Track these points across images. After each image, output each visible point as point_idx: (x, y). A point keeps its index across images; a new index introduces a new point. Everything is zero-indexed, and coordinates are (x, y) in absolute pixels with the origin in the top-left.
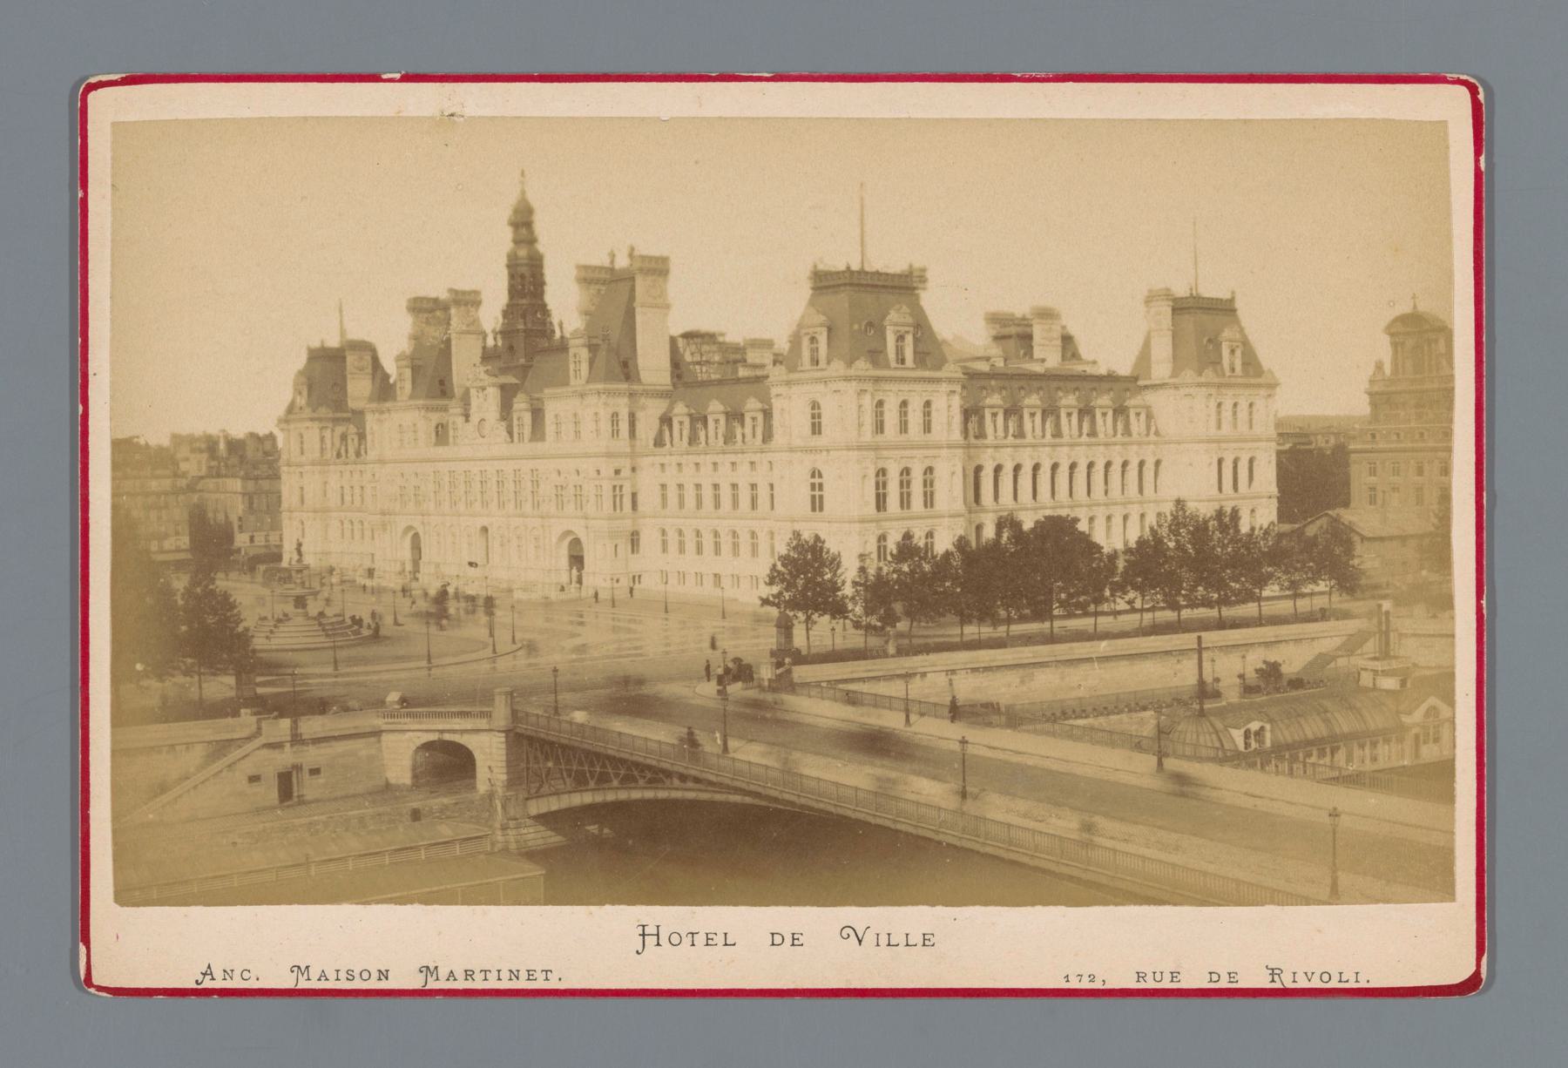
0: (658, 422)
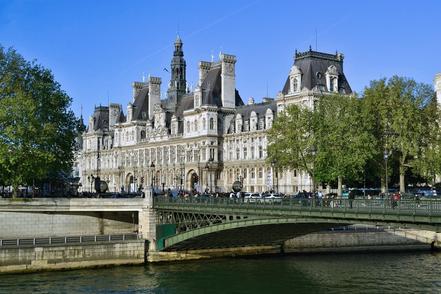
0: (230, 123)
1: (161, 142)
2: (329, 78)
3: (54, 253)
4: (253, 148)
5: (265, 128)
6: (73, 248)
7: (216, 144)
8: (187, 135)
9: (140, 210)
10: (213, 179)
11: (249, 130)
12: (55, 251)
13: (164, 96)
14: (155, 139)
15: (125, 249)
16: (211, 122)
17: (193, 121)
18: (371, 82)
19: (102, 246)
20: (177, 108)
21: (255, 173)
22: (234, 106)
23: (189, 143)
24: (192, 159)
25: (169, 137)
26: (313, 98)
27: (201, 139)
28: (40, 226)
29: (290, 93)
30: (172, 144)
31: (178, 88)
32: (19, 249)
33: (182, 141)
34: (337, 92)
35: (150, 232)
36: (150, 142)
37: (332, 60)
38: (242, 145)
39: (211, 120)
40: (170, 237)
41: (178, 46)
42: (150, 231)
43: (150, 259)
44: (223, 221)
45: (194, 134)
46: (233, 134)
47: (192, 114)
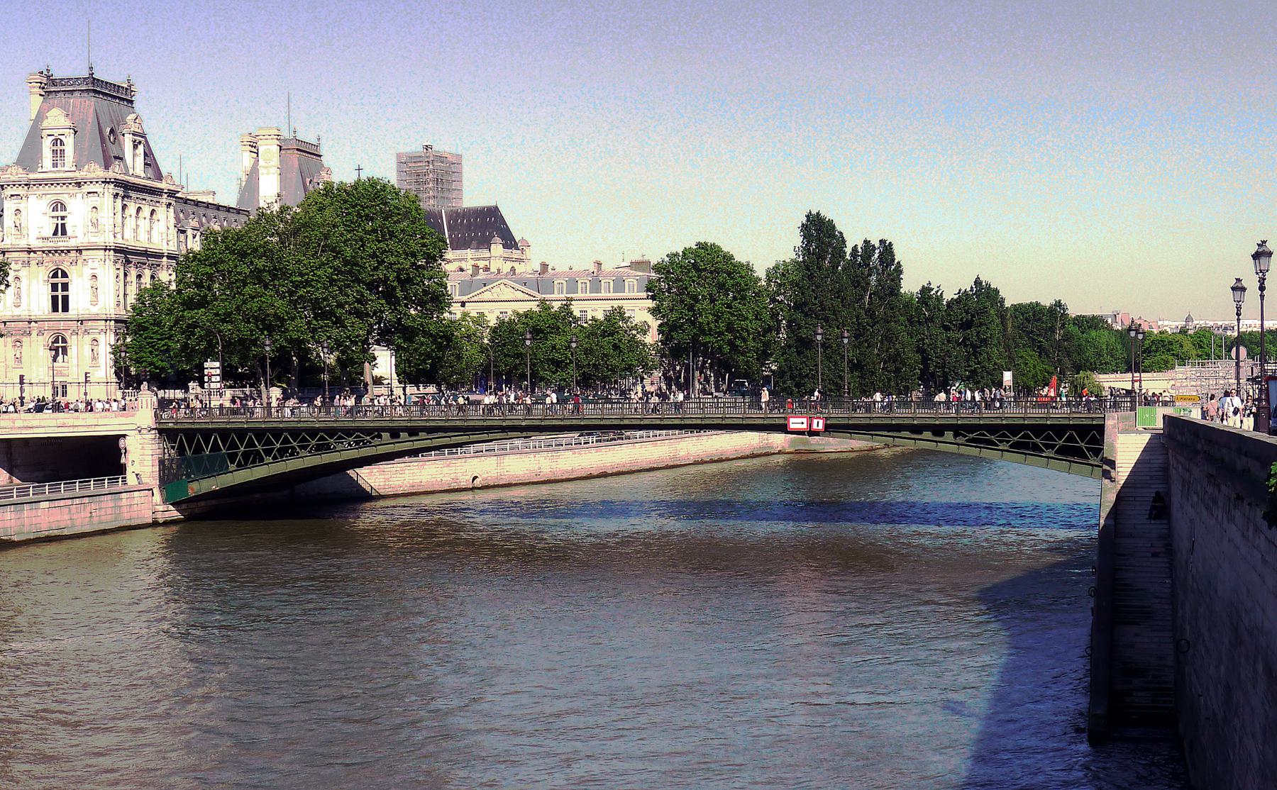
29: (43, 170)
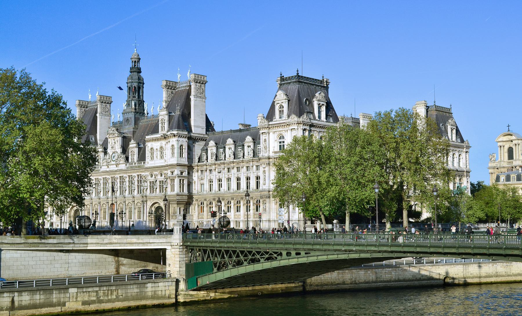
1: (116, 171)
2: (317, 105)
3: (88, 294)
4: (229, 179)
5: (244, 157)
6: (106, 288)
7: (185, 174)
8: (149, 163)
9: (168, 247)
10: (182, 213)
11: (225, 159)
12: (89, 292)
13: (117, 116)
14: (108, 167)
15: (157, 289)
16: (180, 149)
17: (158, 148)
18: (376, 113)
19: (135, 286)
20: (134, 132)
21: (232, 207)
22: (204, 131)
23: (152, 172)
24: (156, 191)
25: (126, 165)
26: (302, 127)
27: (169, 169)
28: (56, 266)
29: (276, 120)
30: (131, 173)
31: (135, 109)
32: (54, 290)
33: (144, 170)
34: (325, 120)
35: (180, 271)
36: (102, 170)
37: (319, 86)
38: (216, 176)
39: (180, 147)
40: (206, 275)
41: (135, 62)
42: (180, 269)
43: (181, 299)
44: (279, 258)
45: (158, 162)
46: (205, 163)
47: (157, 140)
